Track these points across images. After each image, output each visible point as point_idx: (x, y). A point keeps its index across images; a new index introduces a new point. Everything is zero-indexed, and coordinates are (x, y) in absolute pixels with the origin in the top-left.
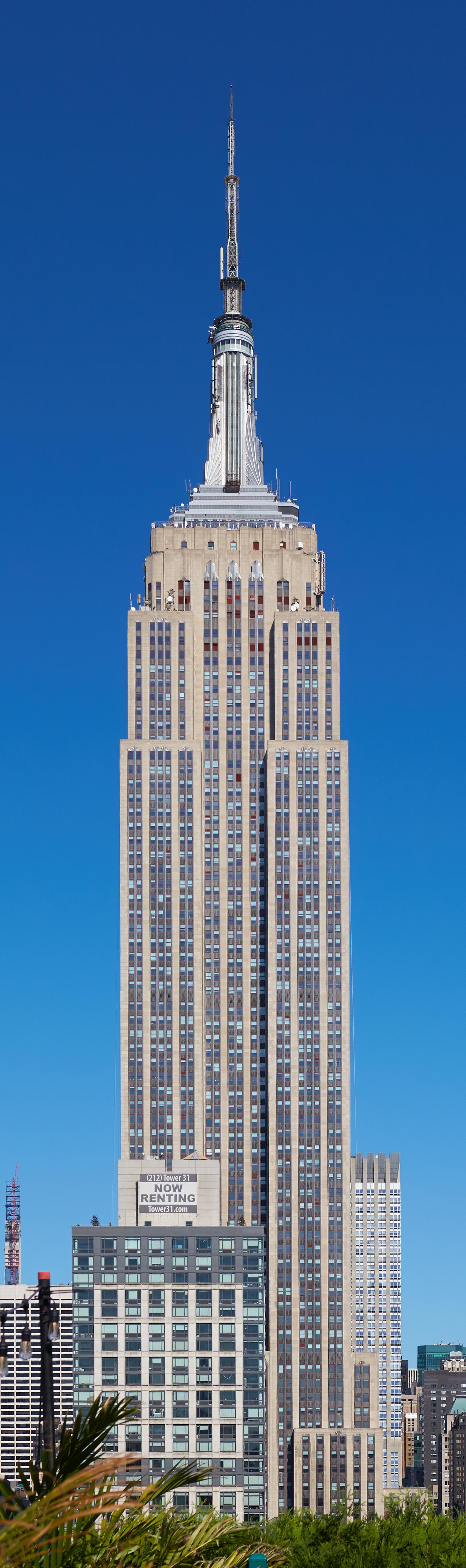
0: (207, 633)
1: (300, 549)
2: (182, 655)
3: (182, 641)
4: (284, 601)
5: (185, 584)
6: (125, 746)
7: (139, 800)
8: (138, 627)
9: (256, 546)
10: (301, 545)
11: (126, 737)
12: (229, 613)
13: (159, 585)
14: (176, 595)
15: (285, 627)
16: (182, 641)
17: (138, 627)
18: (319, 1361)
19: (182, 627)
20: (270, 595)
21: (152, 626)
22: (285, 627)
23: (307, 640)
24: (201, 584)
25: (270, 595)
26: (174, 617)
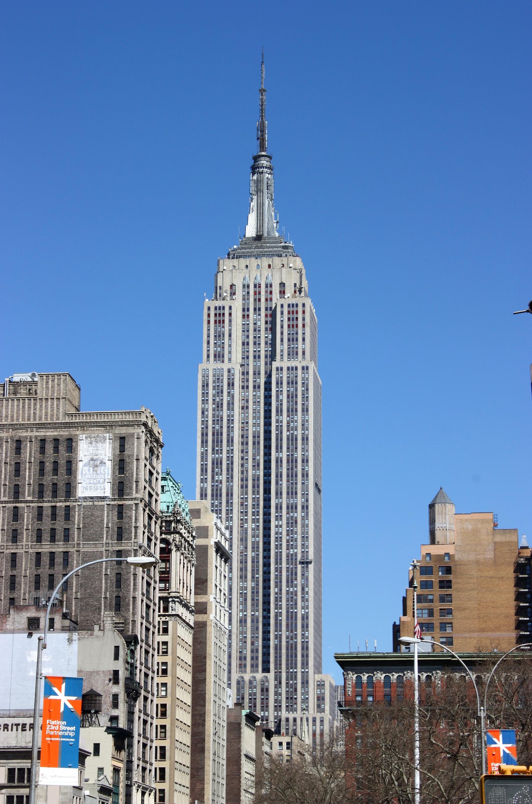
0: (244, 310)
1: (290, 267)
2: (230, 321)
3: (230, 314)
4: (282, 293)
5: (233, 287)
6: (201, 367)
7: (207, 393)
8: (209, 308)
9: (269, 266)
10: (291, 265)
11: (202, 363)
12: (255, 300)
13: (220, 287)
14: (229, 292)
15: (282, 306)
16: (230, 314)
17: (209, 308)
18: (296, 679)
19: (230, 308)
20: (276, 290)
21: (216, 308)
22: (282, 306)
23: (293, 312)
24: (241, 286)
25: (276, 290)
26: (226, 304)
